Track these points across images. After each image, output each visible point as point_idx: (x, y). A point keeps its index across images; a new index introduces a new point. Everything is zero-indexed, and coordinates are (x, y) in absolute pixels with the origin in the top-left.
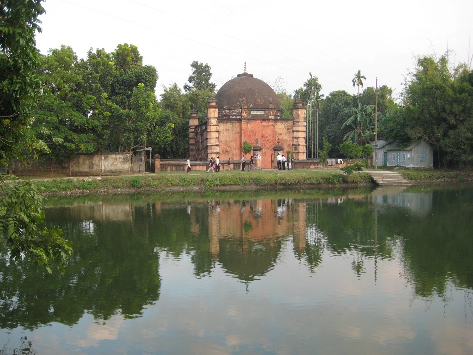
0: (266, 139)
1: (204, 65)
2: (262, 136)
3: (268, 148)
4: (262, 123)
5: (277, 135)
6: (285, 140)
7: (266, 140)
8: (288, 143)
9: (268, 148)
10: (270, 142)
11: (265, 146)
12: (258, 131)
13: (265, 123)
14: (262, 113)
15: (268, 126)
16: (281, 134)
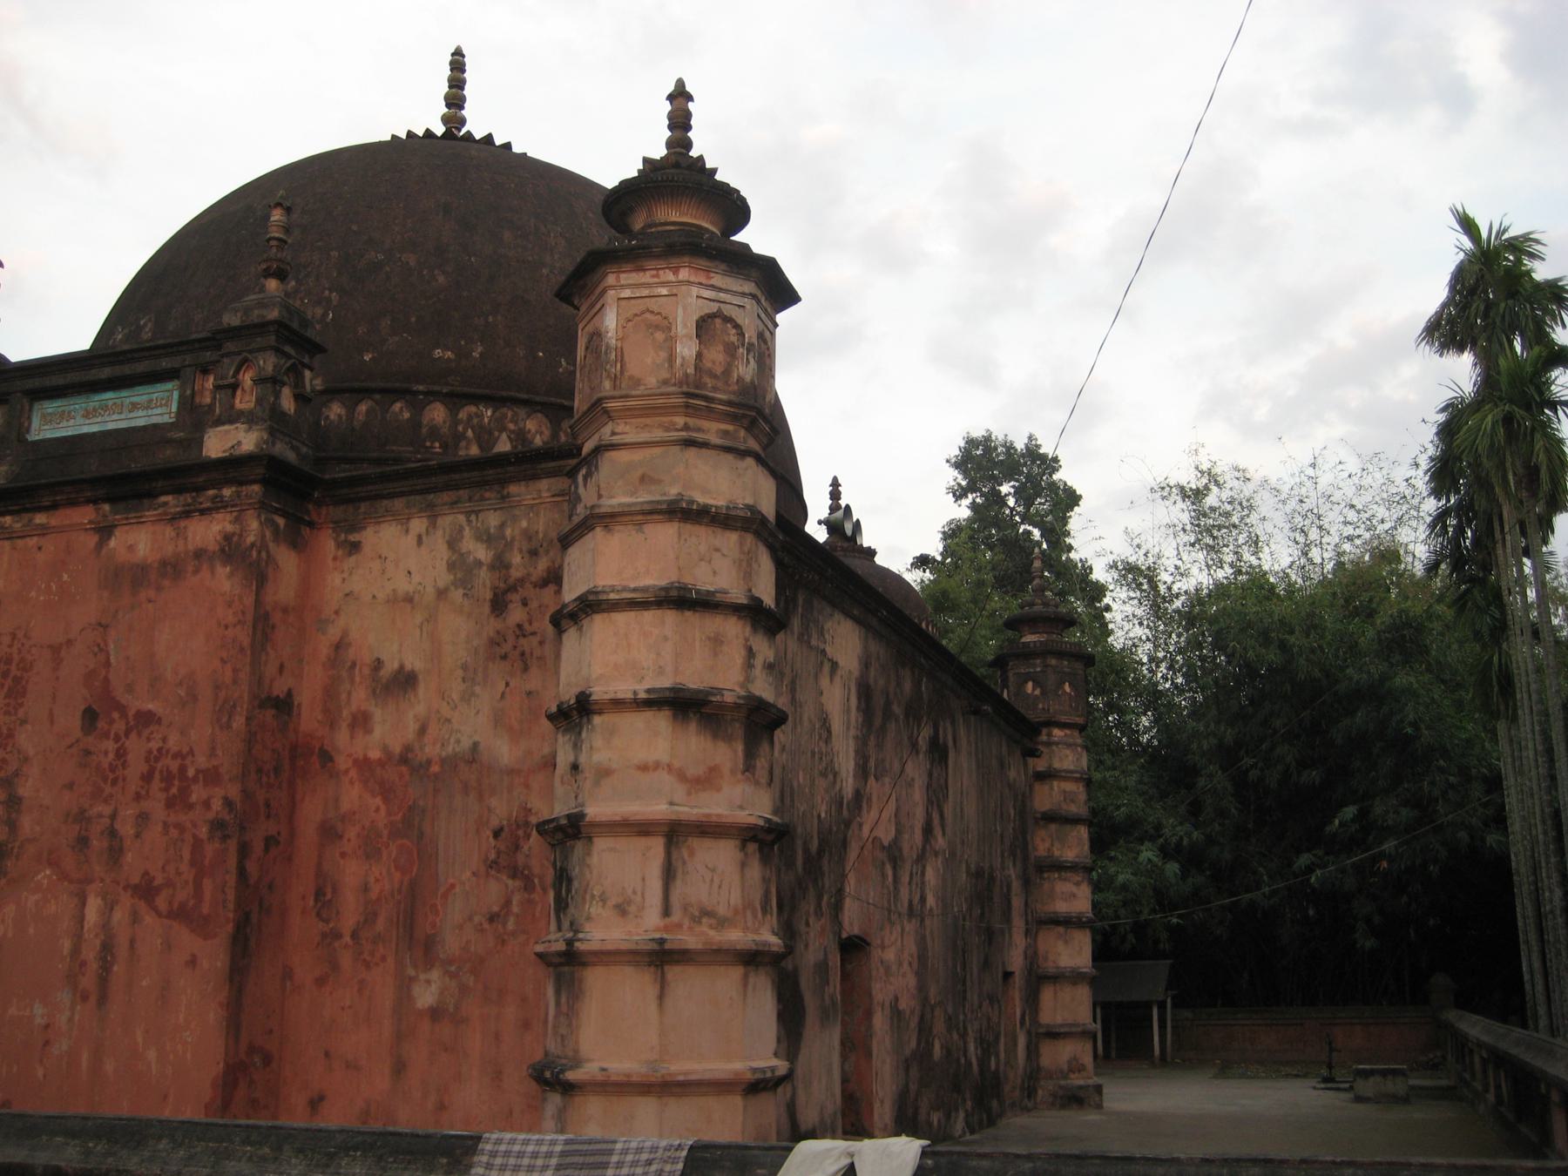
0: (136, 747)
1: (1020, 445)
2: (90, 716)
3: (146, 891)
4: (105, 531)
5: (359, 697)
6: (451, 763)
7: (136, 766)
8: (501, 809)
9: (146, 891)
10: (177, 802)
11: (115, 853)
12: (56, 650)
13: (140, 541)
14: (151, 407)
15: (171, 569)
16: (405, 681)
